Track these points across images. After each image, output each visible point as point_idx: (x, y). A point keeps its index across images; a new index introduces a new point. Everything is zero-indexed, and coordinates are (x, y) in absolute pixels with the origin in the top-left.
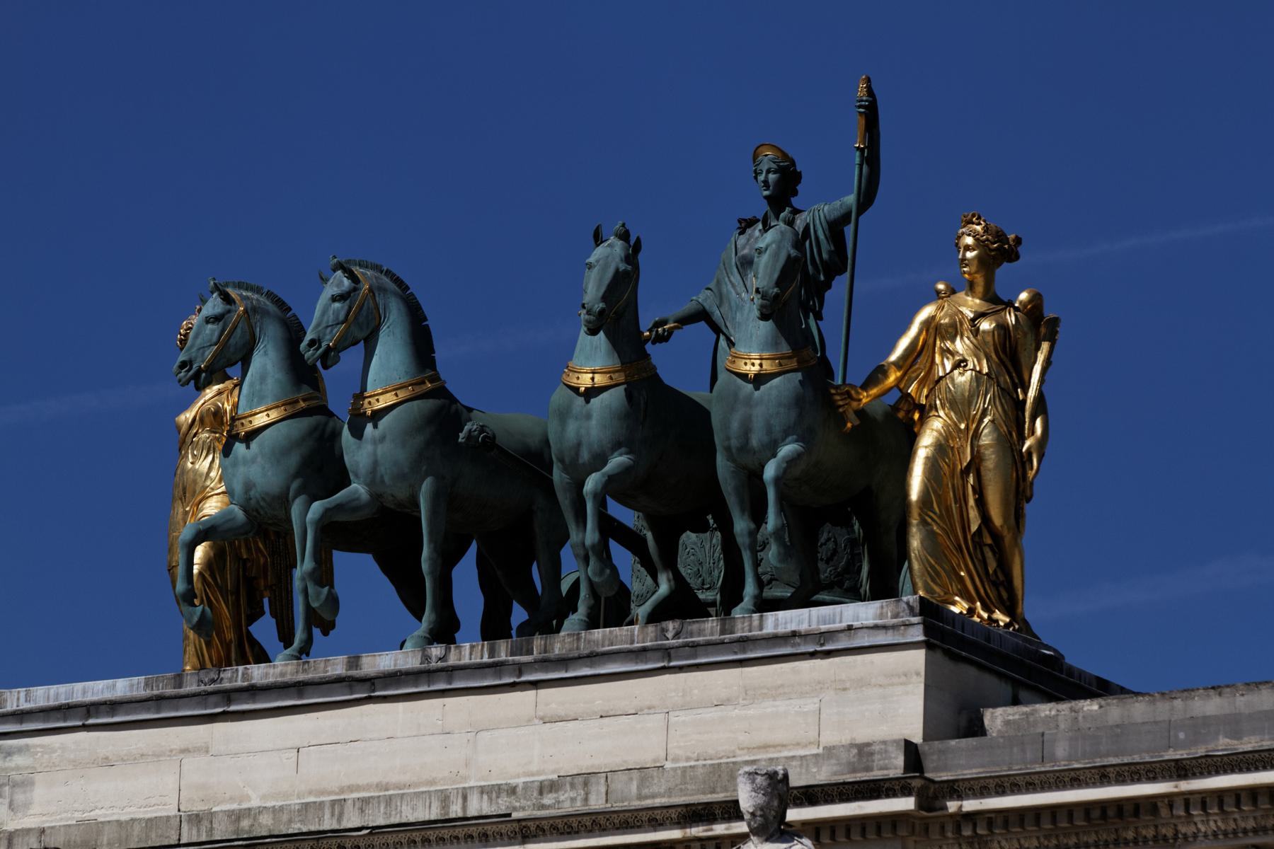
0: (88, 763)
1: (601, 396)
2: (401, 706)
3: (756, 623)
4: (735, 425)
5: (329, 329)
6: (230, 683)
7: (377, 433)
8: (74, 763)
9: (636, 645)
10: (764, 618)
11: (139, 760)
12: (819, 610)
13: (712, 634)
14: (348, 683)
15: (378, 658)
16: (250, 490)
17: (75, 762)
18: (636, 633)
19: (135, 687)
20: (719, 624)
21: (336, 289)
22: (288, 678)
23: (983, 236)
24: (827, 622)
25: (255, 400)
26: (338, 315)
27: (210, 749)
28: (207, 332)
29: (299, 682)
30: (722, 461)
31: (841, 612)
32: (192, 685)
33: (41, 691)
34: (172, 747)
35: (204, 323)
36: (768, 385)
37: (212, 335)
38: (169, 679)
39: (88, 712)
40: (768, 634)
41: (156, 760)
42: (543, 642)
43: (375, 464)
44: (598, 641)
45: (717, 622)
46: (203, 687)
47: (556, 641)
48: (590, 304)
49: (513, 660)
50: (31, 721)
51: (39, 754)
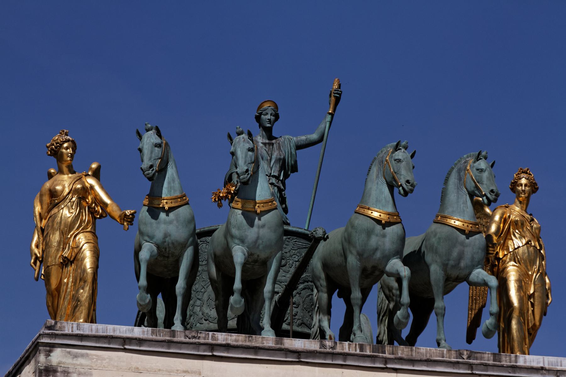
0: (126, 369)
1: (392, 227)
2: (317, 369)
3: (513, 359)
4: (455, 254)
5: (249, 165)
6: (204, 340)
7: (261, 223)
8: (117, 368)
9: (445, 359)
10: (518, 357)
11: (157, 372)
12: (548, 358)
13: (489, 360)
14: (285, 352)
15: (293, 341)
16: (167, 237)
17: (117, 367)
18: (445, 353)
19: (146, 333)
20: (492, 356)
21: (248, 144)
22: (240, 343)
23: (533, 181)
24: (554, 365)
25: (172, 191)
26: (252, 158)
27: (202, 373)
28: (156, 151)
29: (256, 347)
30: (439, 270)
31: (561, 361)
32: (181, 337)
33: (87, 325)
34: (178, 369)
35: (154, 147)
36: (473, 237)
37: (159, 153)
38: (166, 331)
39: (125, 341)
40: (520, 366)
41: (168, 374)
42: (391, 349)
43: (258, 238)
44: (423, 354)
45: (491, 355)
46: (187, 340)
47: (399, 349)
48: (412, 181)
49: (382, 356)
50: (88, 341)
51: (95, 360)
